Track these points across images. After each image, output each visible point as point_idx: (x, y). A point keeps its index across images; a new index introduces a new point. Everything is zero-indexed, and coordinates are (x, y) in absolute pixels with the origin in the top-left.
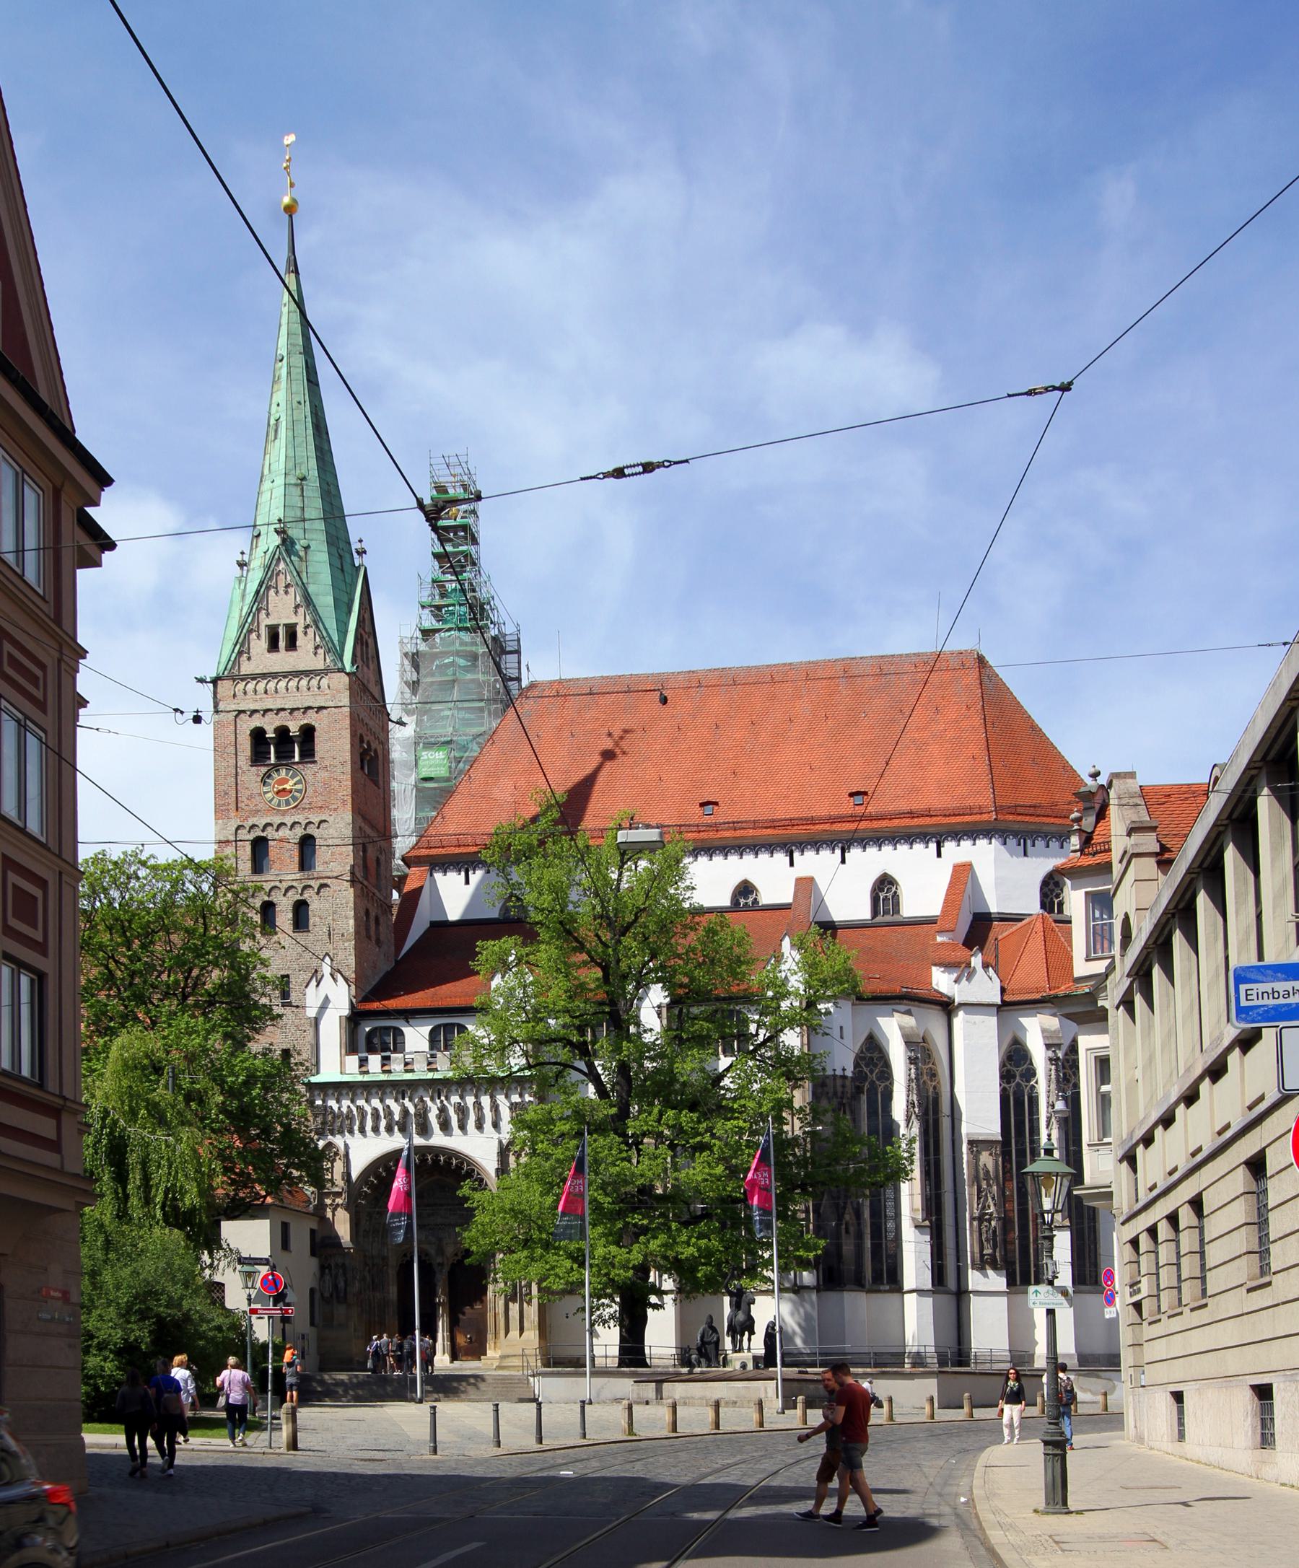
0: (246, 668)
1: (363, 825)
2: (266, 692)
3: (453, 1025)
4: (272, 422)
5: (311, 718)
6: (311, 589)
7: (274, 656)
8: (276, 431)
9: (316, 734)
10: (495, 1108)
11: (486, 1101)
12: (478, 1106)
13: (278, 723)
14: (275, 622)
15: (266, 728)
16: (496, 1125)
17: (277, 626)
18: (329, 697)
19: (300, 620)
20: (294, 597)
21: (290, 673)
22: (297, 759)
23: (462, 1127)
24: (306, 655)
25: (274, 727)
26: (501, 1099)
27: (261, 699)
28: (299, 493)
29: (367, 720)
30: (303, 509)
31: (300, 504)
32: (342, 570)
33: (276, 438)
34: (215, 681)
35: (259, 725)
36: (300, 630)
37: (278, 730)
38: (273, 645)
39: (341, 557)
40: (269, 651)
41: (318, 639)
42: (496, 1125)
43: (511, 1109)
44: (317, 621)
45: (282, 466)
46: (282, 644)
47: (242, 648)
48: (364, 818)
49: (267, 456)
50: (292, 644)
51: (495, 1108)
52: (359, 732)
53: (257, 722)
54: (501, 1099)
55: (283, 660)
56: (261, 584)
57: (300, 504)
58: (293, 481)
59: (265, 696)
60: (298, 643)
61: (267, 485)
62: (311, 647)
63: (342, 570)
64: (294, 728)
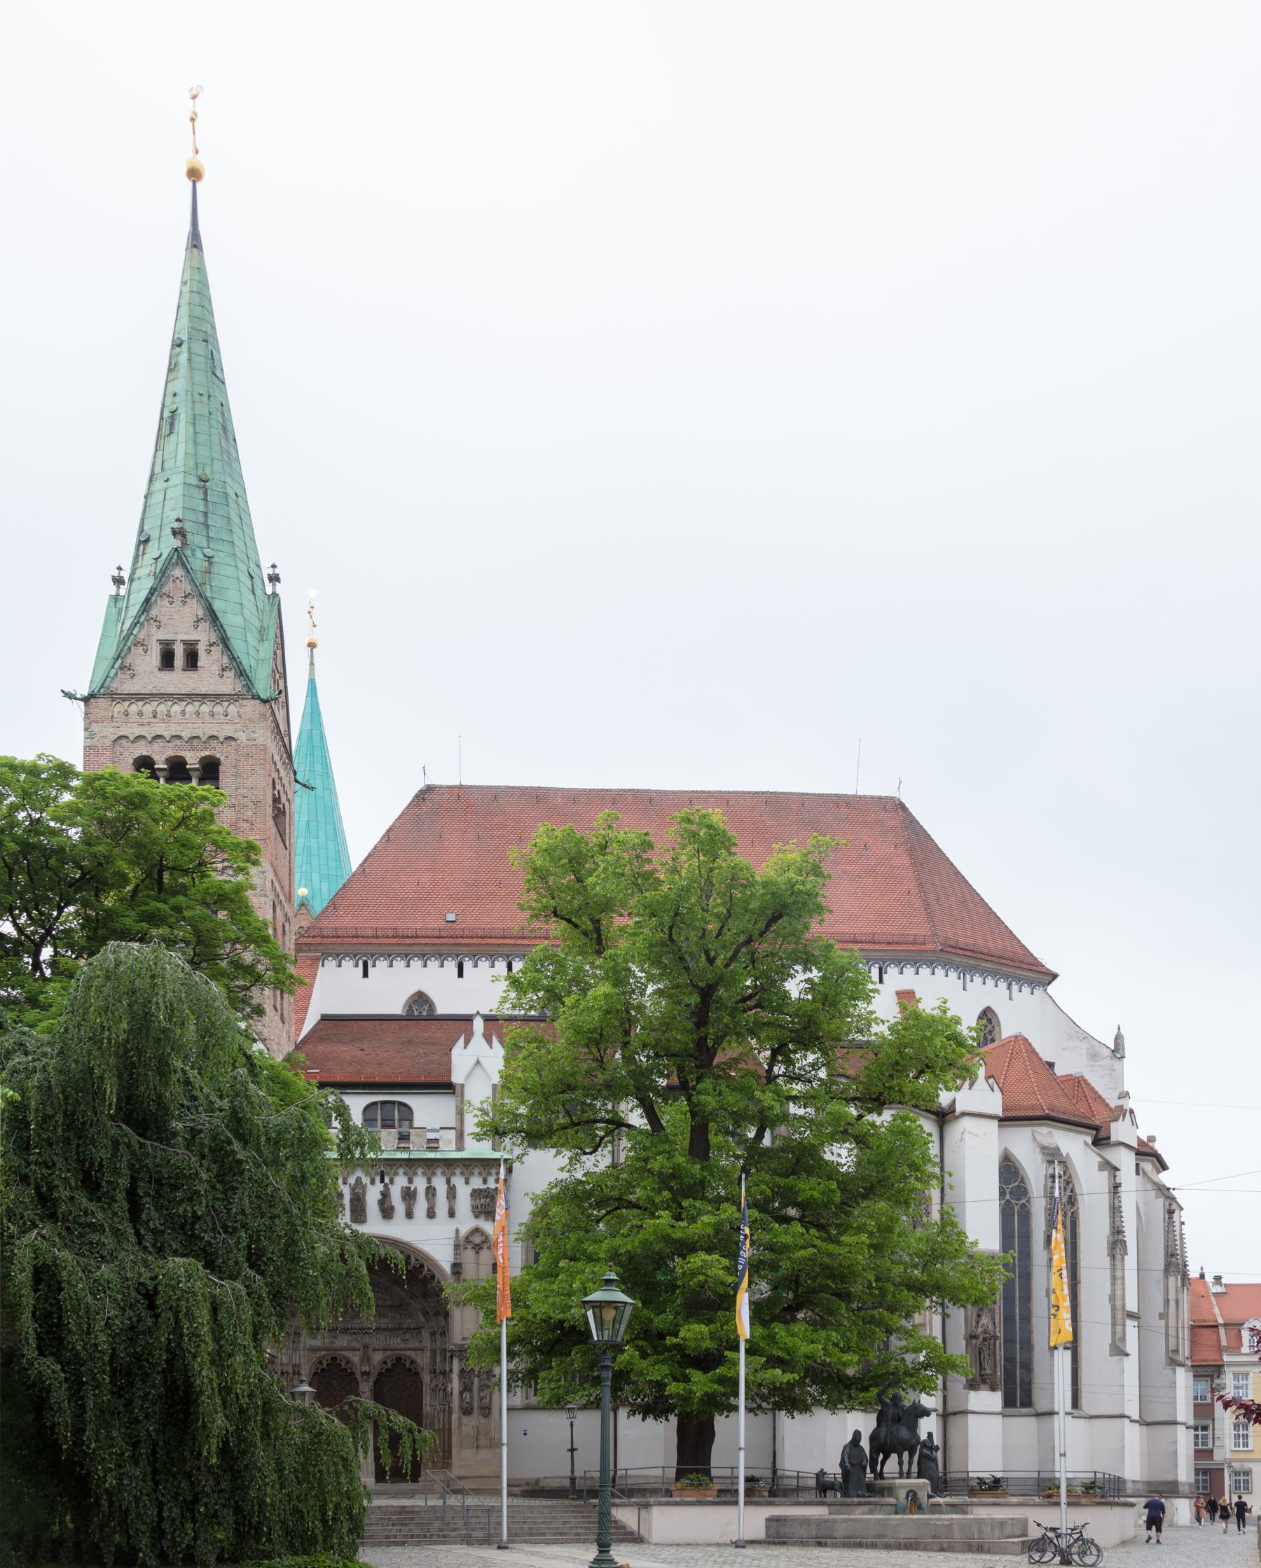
0: (130, 687)
2: (155, 716)
3: (393, 1103)
4: (167, 414)
5: (217, 751)
6: (217, 605)
7: (167, 676)
8: (172, 425)
9: (221, 768)
10: (452, 1193)
11: (439, 1183)
12: (431, 1192)
13: (171, 753)
14: (170, 637)
15: (155, 757)
16: (452, 1214)
17: (173, 641)
18: (238, 726)
19: (203, 636)
20: (195, 608)
21: (190, 696)
23: (409, 1214)
24: (210, 676)
25: (164, 757)
26: (458, 1181)
27: (149, 723)
30: (206, 514)
31: (202, 509)
33: (171, 432)
34: (86, 700)
35: (145, 753)
36: (201, 649)
37: (168, 761)
38: (167, 660)
40: (160, 670)
41: (226, 660)
42: (452, 1214)
43: (472, 1195)
44: (225, 641)
45: (180, 462)
46: (179, 660)
47: (121, 661)
49: (160, 453)
51: (452, 1193)
53: (142, 750)
54: (458, 1181)
55: (179, 680)
56: (152, 591)
57: (202, 509)
58: (194, 481)
59: (153, 720)
61: (159, 485)
62: (216, 668)
64: (192, 760)
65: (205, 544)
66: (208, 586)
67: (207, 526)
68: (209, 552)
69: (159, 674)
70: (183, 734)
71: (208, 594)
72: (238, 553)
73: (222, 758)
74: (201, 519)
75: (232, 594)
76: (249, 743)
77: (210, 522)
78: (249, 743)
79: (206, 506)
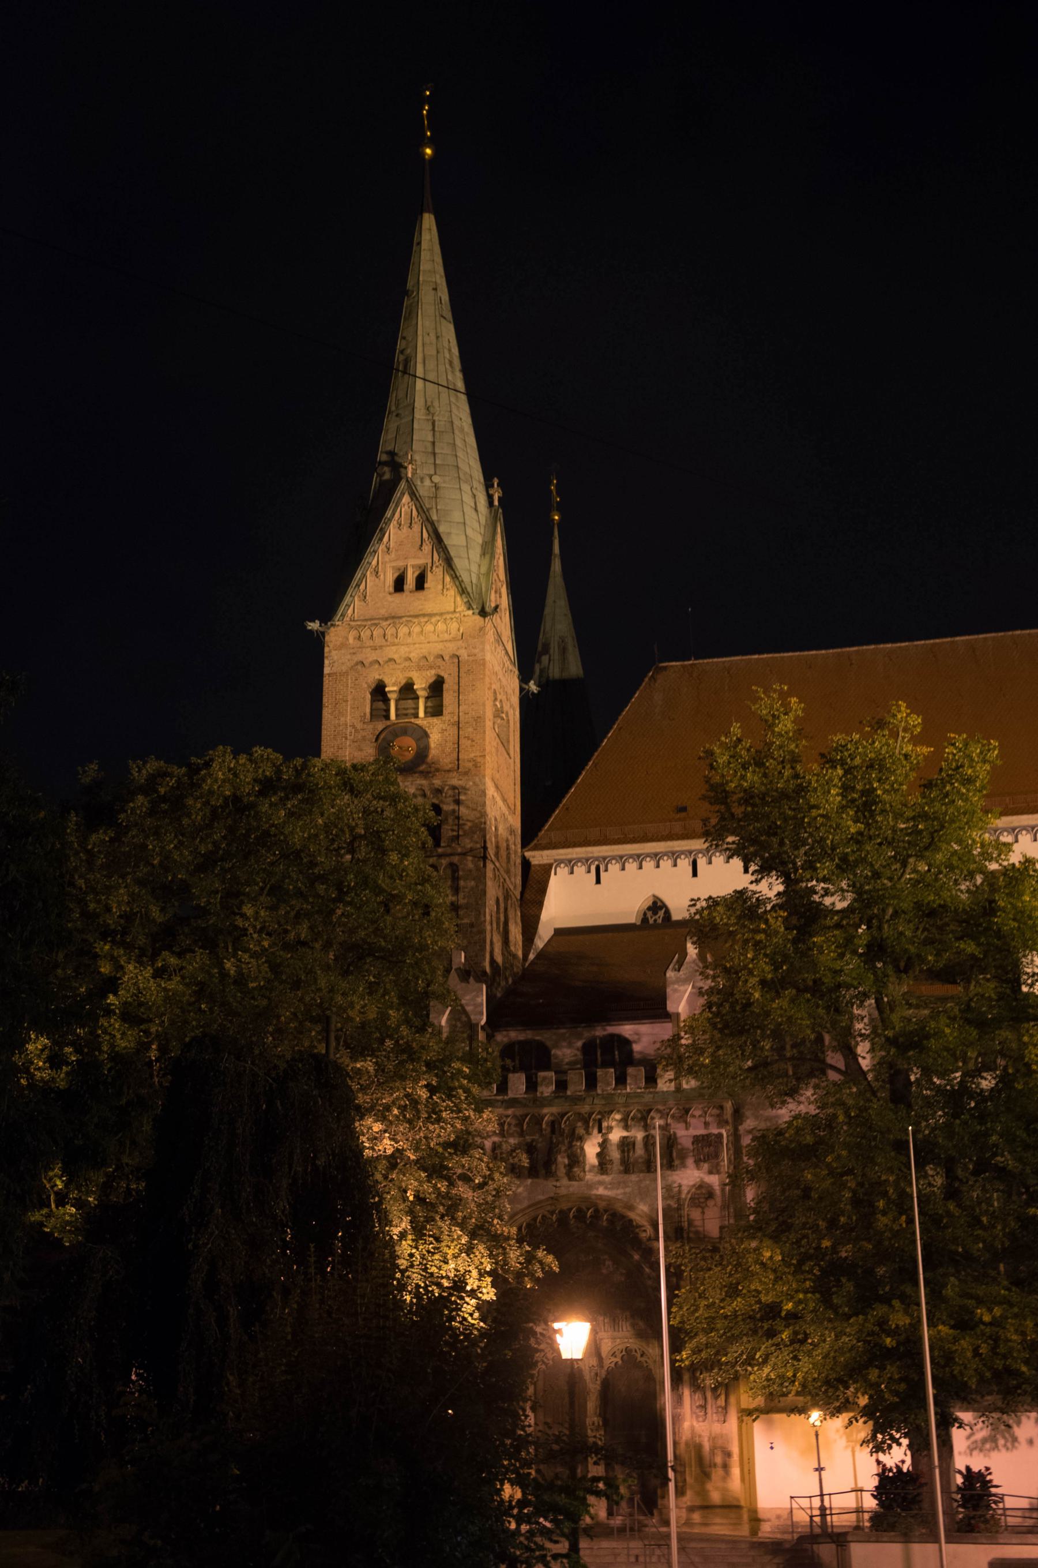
1: (495, 794)
6: (442, 529)
22: (421, 714)
28: (431, 427)
29: (501, 676)
30: (433, 443)
32: (476, 510)
39: (474, 496)
48: (497, 787)
50: (420, 583)
52: (494, 686)
57: (431, 439)
60: (426, 585)
63: (476, 510)
65: (432, 472)
66: (435, 511)
67: (434, 454)
68: (436, 479)
69: (390, 598)
70: (411, 656)
71: (435, 518)
72: (461, 475)
73: (446, 677)
74: (430, 450)
75: (457, 516)
76: (471, 658)
77: (437, 451)
78: (471, 658)
79: (434, 435)
